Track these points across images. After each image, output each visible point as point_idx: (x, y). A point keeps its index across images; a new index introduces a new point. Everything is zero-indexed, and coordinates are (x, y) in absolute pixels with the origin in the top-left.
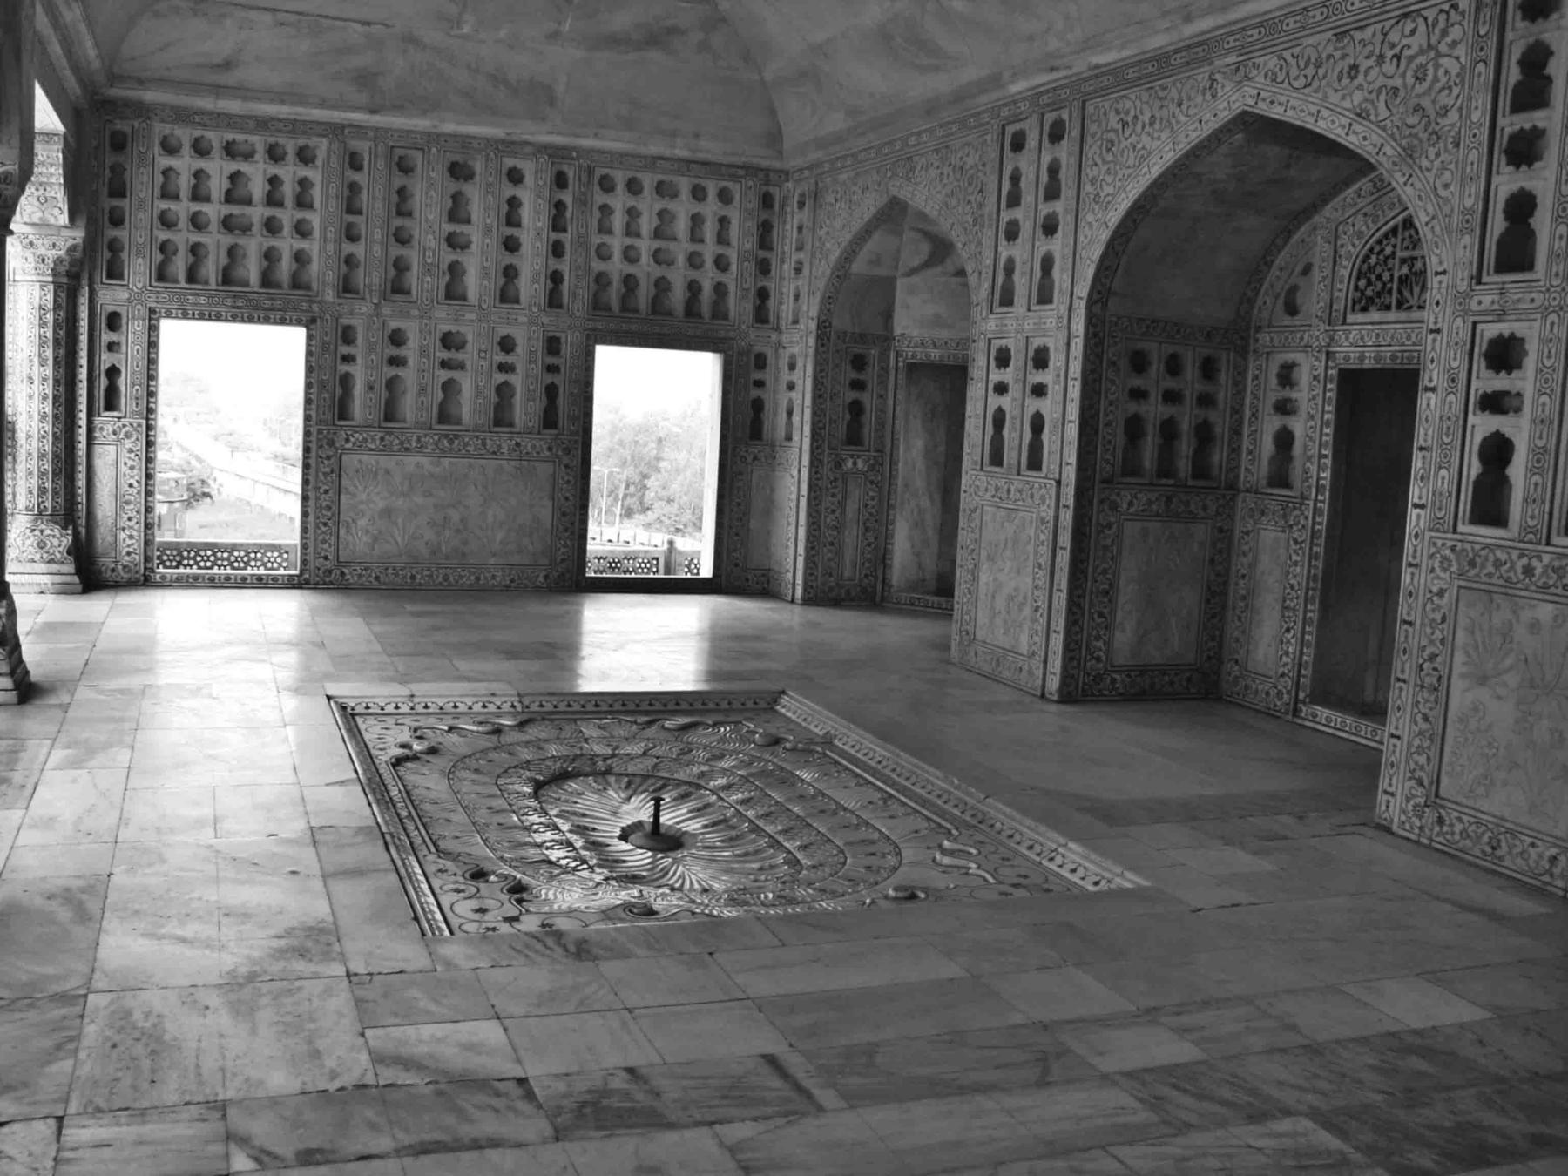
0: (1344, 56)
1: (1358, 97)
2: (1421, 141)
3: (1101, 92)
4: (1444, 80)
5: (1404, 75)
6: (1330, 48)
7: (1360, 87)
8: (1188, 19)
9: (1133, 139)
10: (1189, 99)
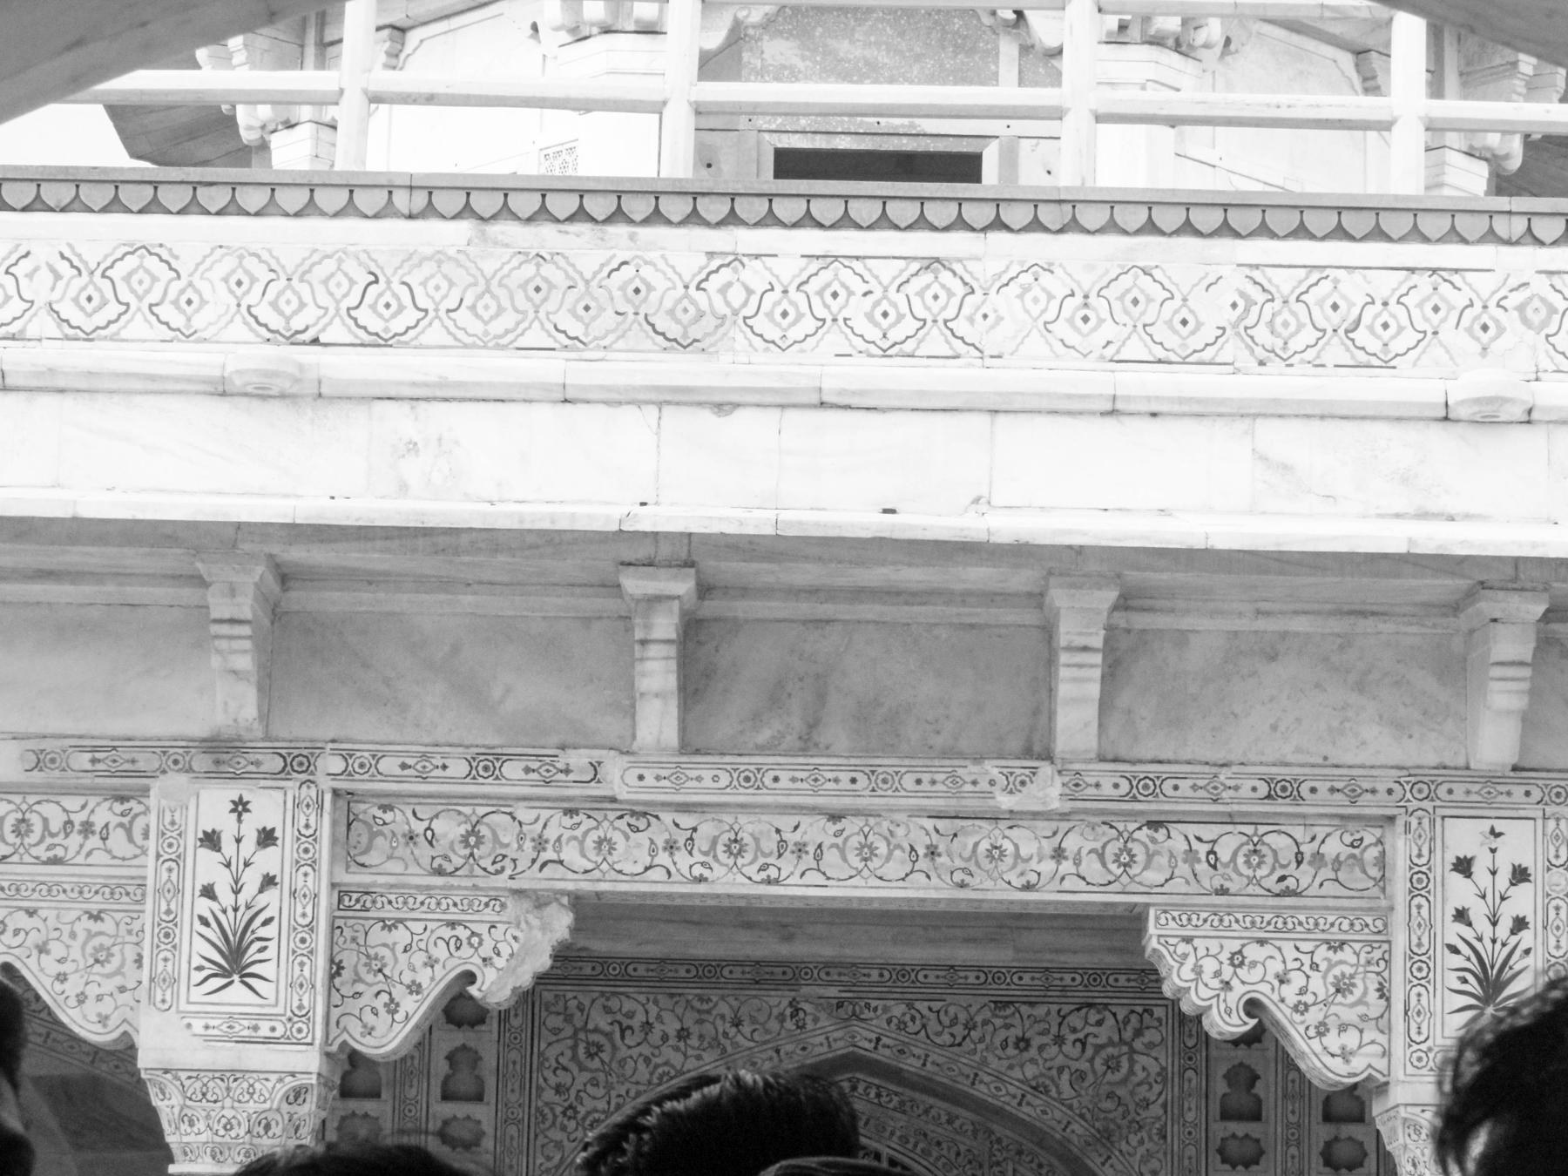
0: (1007, 1027)
1: (1030, 1071)
2: (1119, 1127)
3: (581, 981)
4: (1141, 1075)
5: (1091, 1060)
6: (987, 1014)
7: (1032, 1061)
8: (789, 938)
9: (645, 1050)
10: (753, 1020)
